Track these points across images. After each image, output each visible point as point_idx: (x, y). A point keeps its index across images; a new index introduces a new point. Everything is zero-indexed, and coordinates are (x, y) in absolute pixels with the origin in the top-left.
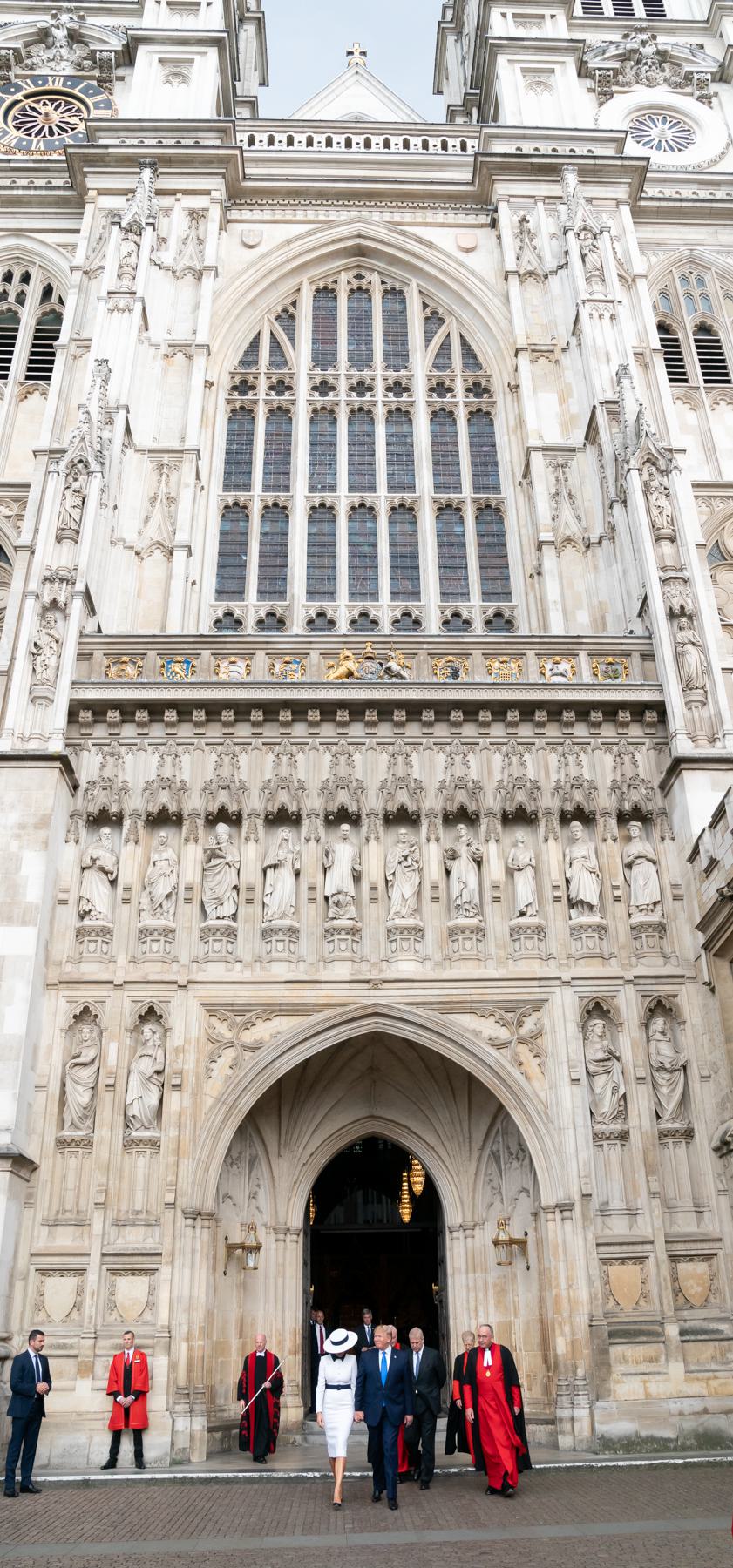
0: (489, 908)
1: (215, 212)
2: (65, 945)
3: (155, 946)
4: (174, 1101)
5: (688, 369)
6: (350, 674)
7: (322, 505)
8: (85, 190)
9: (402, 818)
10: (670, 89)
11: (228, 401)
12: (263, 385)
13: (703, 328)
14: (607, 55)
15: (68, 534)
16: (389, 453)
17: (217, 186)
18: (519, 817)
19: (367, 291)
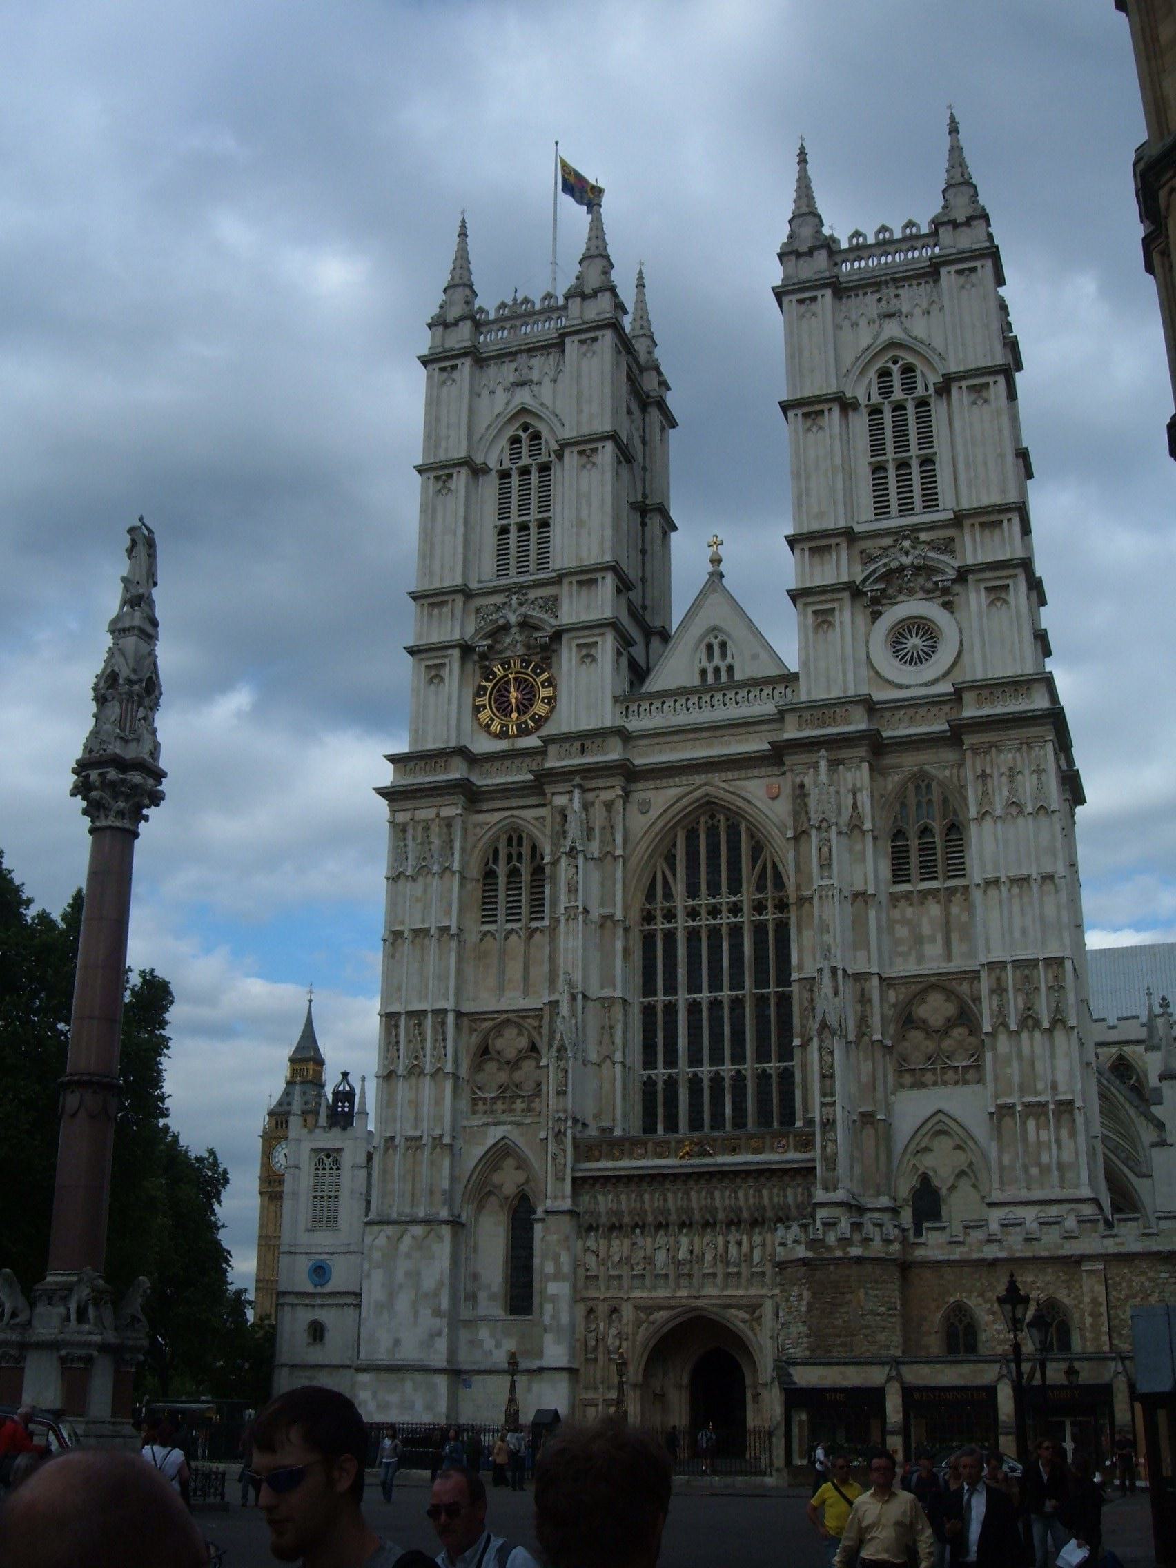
0: (743, 1264)
1: (619, 805)
2: (581, 1284)
3: (615, 1283)
4: (625, 1344)
6: (687, 1153)
7: (695, 1000)
8: (543, 794)
9: (706, 1225)
10: (925, 596)
11: (641, 931)
12: (659, 914)
13: (926, 831)
15: (562, 1093)
16: (731, 960)
17: (618, 782)
18: (755, 1223)
19: (718, 827)
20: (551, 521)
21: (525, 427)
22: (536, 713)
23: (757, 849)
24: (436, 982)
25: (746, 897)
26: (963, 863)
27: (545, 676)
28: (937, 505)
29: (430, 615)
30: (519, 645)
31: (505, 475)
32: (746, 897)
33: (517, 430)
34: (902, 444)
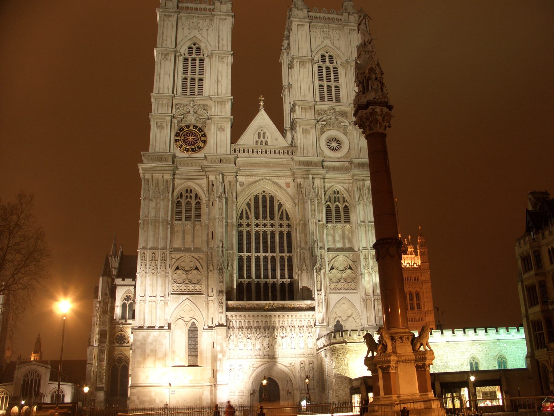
5: (332, 219)
13: (337, 207)
14: (323, 119)
20: (204, 79)
21: (194, 45)
22: (199, 146)
23: (280, 206)
24: (161, 240)
25: (277, 221)
26: (349, 218)
27: (202, 133)
28: (340, 101)
29: (158, 103)
30: (193, 121)
31: (186, 59)
32: (277, 221)
33: (191, 44)
34: (329, 80)
